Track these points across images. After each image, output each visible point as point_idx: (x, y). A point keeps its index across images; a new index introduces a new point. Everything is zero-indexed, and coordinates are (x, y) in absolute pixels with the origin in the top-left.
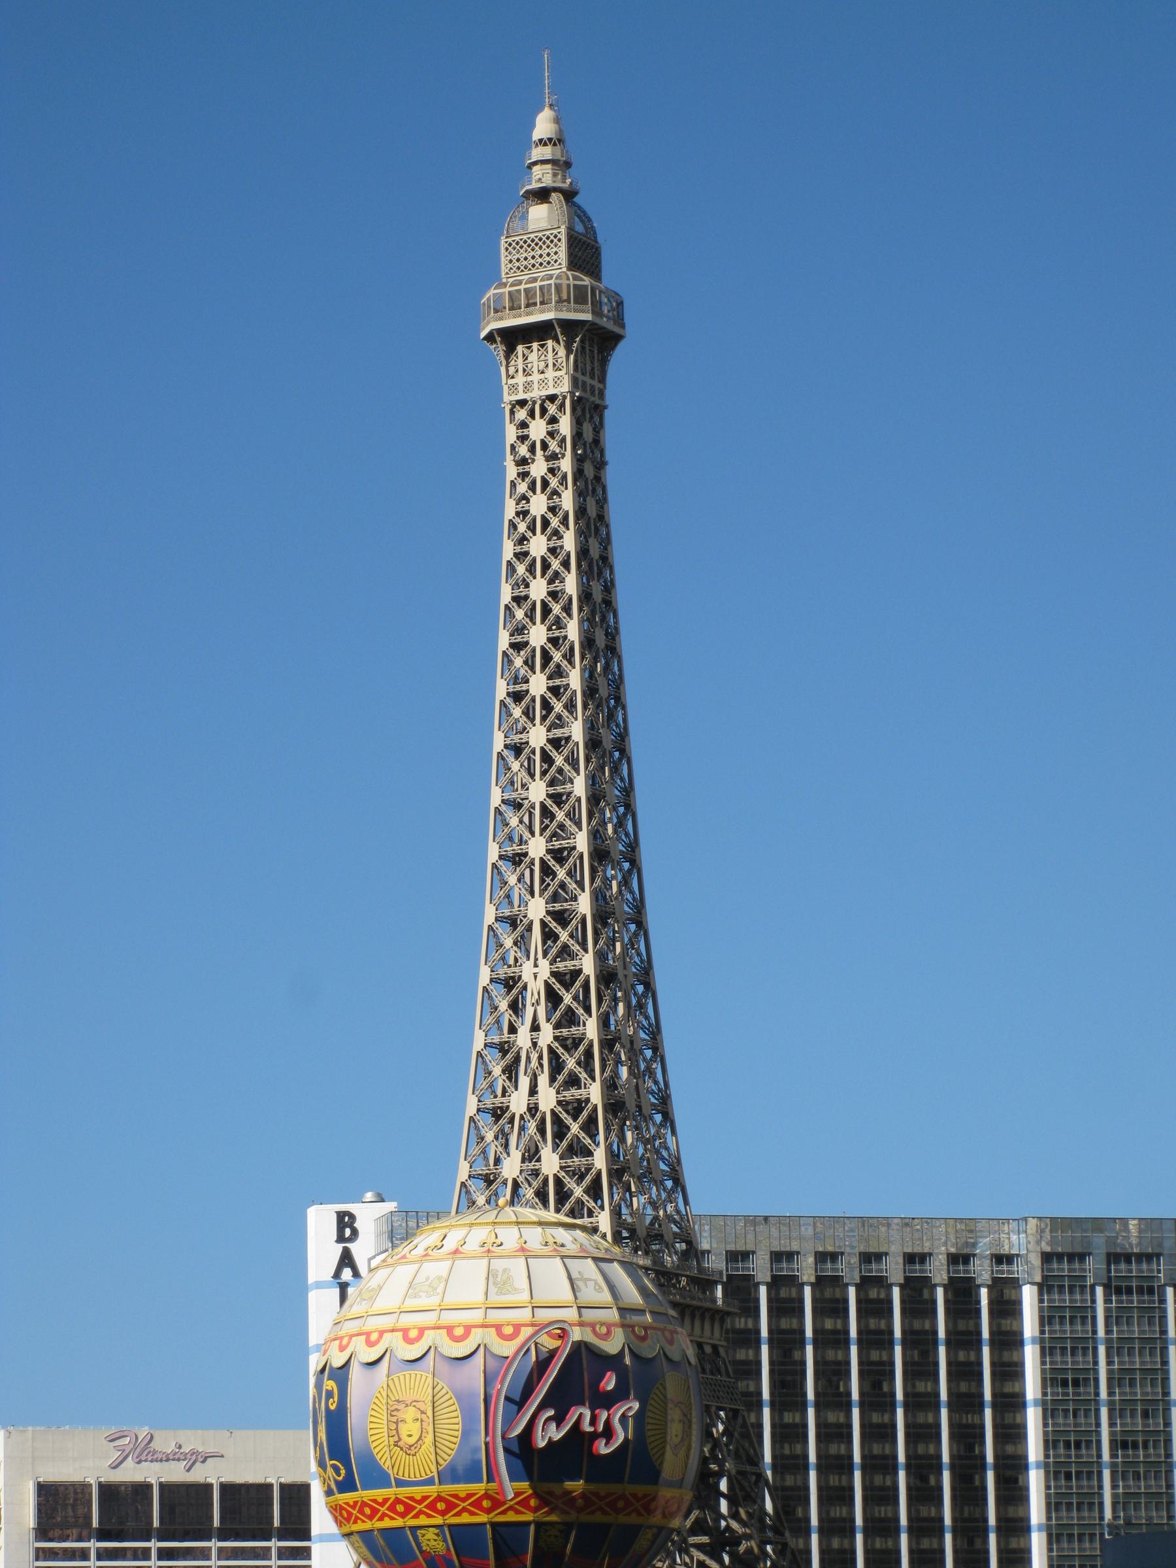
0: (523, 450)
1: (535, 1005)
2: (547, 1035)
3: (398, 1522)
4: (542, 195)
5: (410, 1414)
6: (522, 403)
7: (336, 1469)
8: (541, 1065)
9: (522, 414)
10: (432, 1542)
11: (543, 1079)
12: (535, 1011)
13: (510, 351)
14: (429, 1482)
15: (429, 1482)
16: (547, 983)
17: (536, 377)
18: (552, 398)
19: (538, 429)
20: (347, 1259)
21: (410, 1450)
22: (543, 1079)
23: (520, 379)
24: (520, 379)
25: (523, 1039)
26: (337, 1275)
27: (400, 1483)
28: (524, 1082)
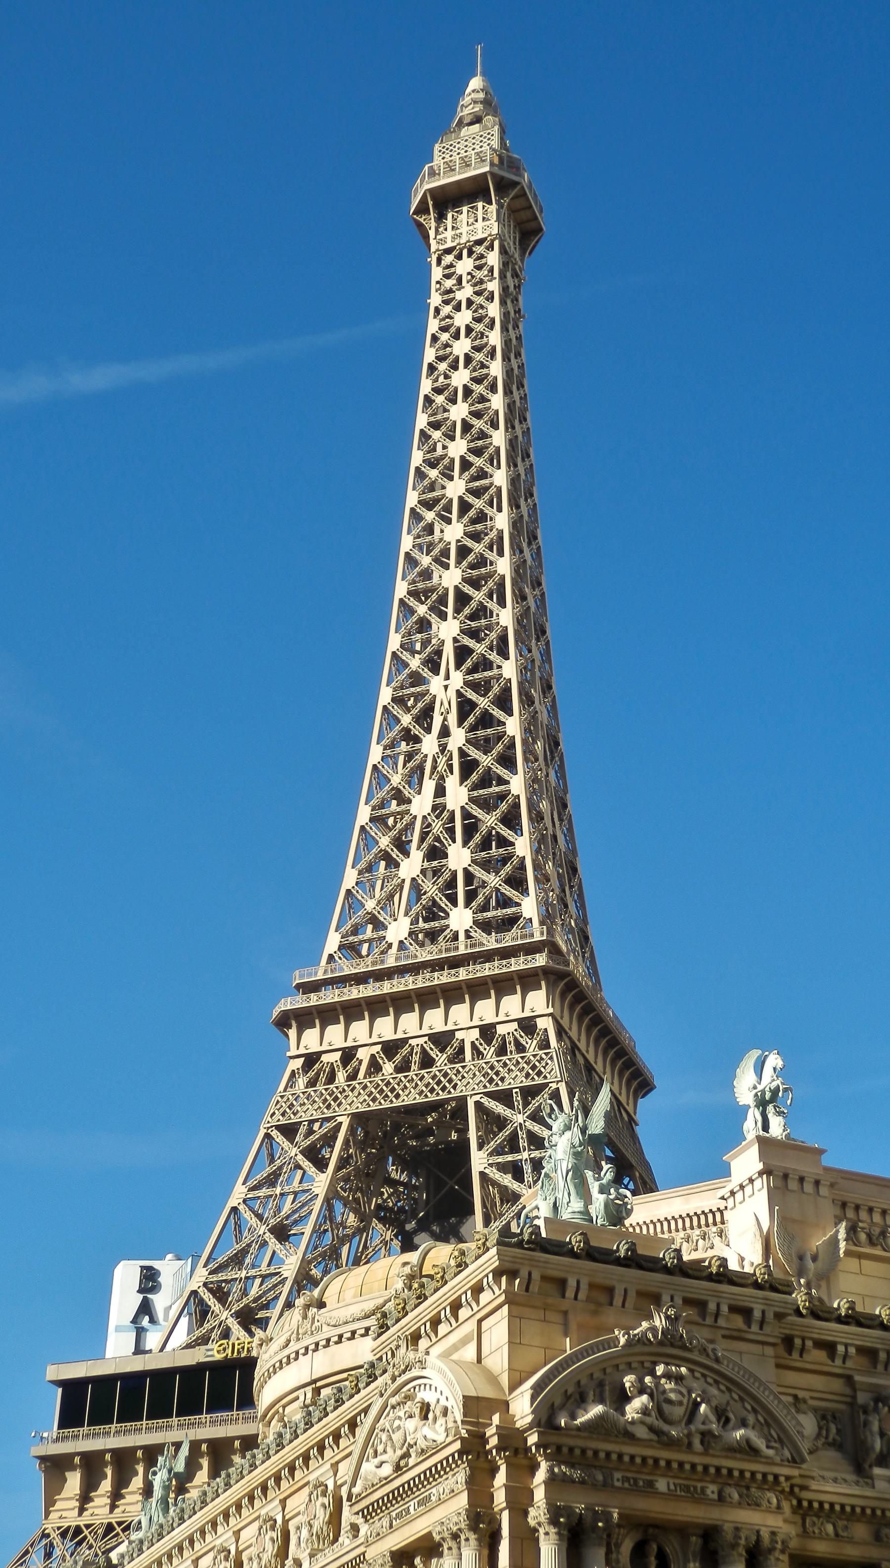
0: (449, 283)
1: (445, 710)
2: (458, 738)
6: (448, 251)
8: (450, 767)
9: (448, 259)
11: (452, 782)
12: (445, 719)
13: (441, 218)
16: (459, 694)
17: (464, 229)
18: (479, 242)
20: (145, 1308)
22: (452, 782)
24: (449, 234)
26: (135, 1321)
28: (429, 786)
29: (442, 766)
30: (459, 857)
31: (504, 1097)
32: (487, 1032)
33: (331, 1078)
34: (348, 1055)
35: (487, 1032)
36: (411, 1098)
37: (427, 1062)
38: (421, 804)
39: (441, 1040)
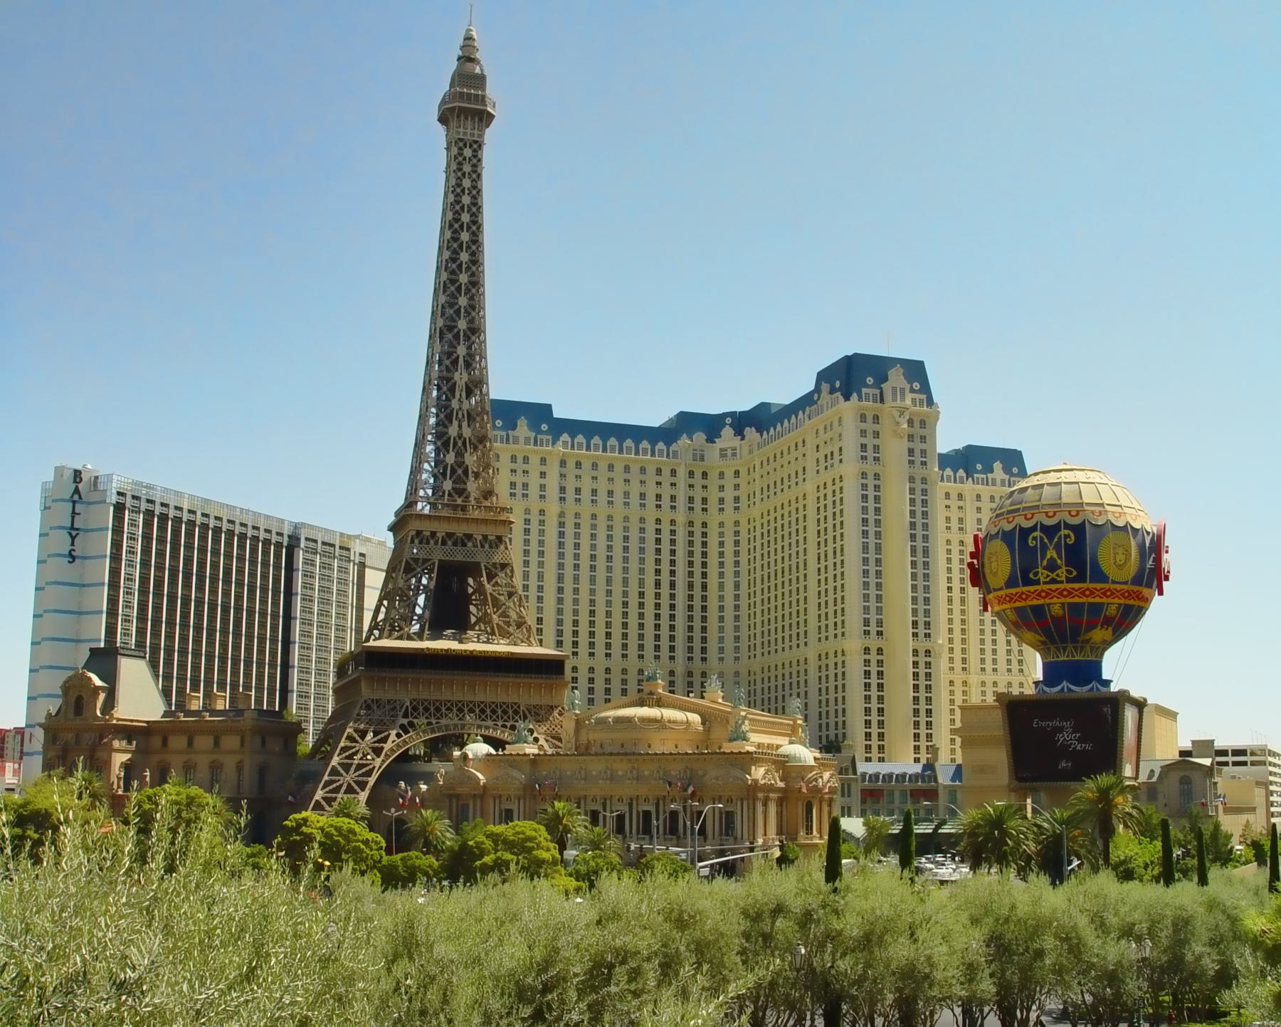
3: (1104, 600)
5: (1120, 551)
6: (461, 140)
7: (1070, 573)
9: (461, 144)
10: (1112, 610)
11: (465, 424)
14: (1126, 583)
15: (1126, 583)
18: (476, 142)
19: (468, 152)
21: (1120, 567)
22: (465, 424)
23: (462, 130)
27: (1114, 582)
28: (455, 423)
33: (428, 543)
34: (433, 534)
35: (485, 537)
36: (460, 558)
37: (464, 545)
38: (453, 431)
39: (469, 537)
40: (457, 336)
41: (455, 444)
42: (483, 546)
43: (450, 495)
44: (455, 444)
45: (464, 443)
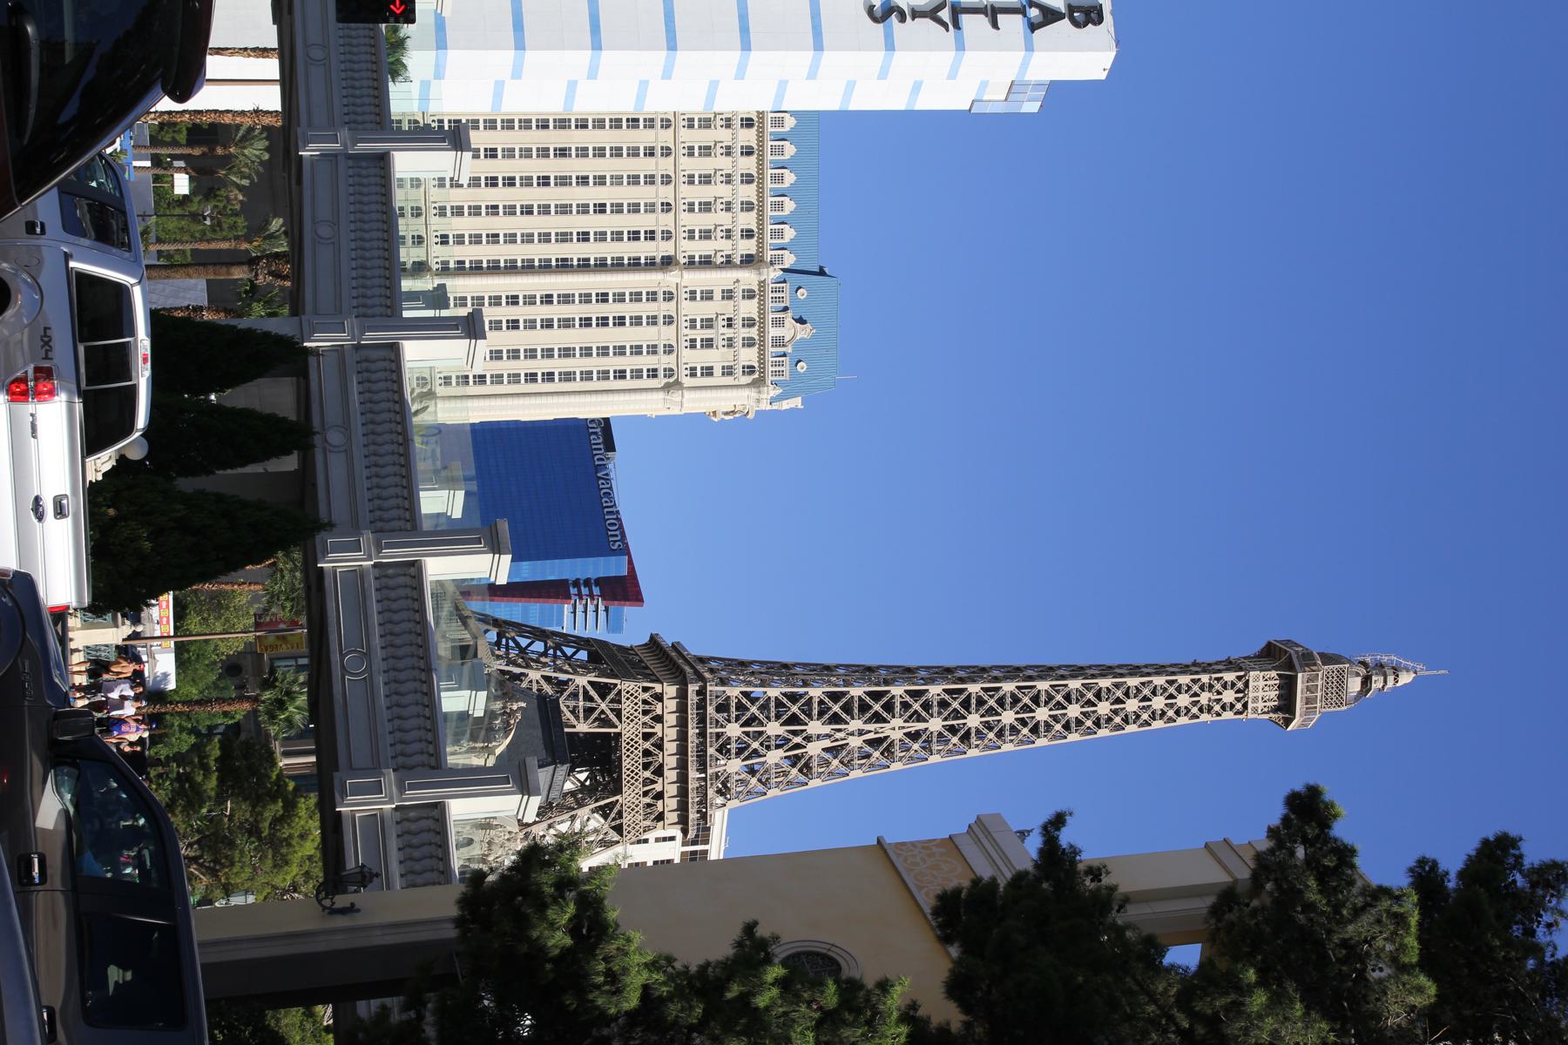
4: (1366, 681)
9: (1240, 685)
11: (827, 743)
18: (1245, 706)
19: (1229, 696)
23: (1262, 683)
24: (1262, 683)
25: (856, 724)
28: (827, 729)
29: (841, 735)
30: (774, 757)
31: (620, 815)
32: (660, 796)
33: (645, 713)
34: (659, 719)
35: (660, 796)
36: (626, 763)
37: (646, 766)
38: (815, 727)
39: (659, 772)
40: (956, 715)
41: (795, 733)
42: (645, 794)
43: (718, 736)
44: (795, 733)
45: (798, 746)
